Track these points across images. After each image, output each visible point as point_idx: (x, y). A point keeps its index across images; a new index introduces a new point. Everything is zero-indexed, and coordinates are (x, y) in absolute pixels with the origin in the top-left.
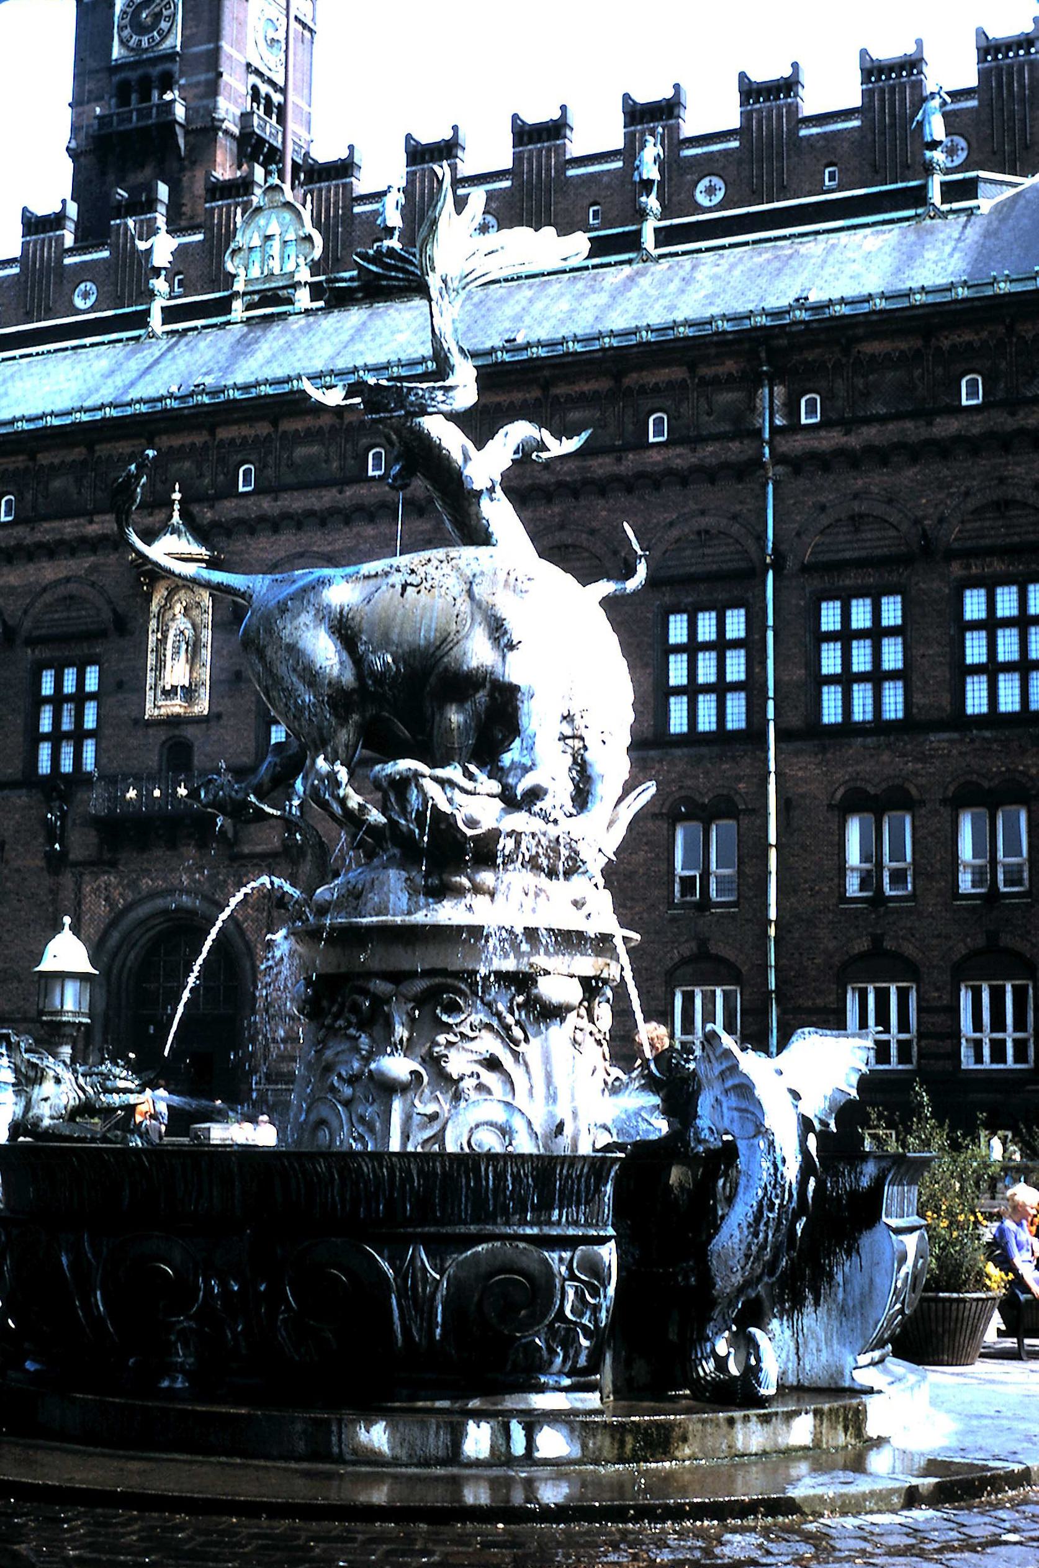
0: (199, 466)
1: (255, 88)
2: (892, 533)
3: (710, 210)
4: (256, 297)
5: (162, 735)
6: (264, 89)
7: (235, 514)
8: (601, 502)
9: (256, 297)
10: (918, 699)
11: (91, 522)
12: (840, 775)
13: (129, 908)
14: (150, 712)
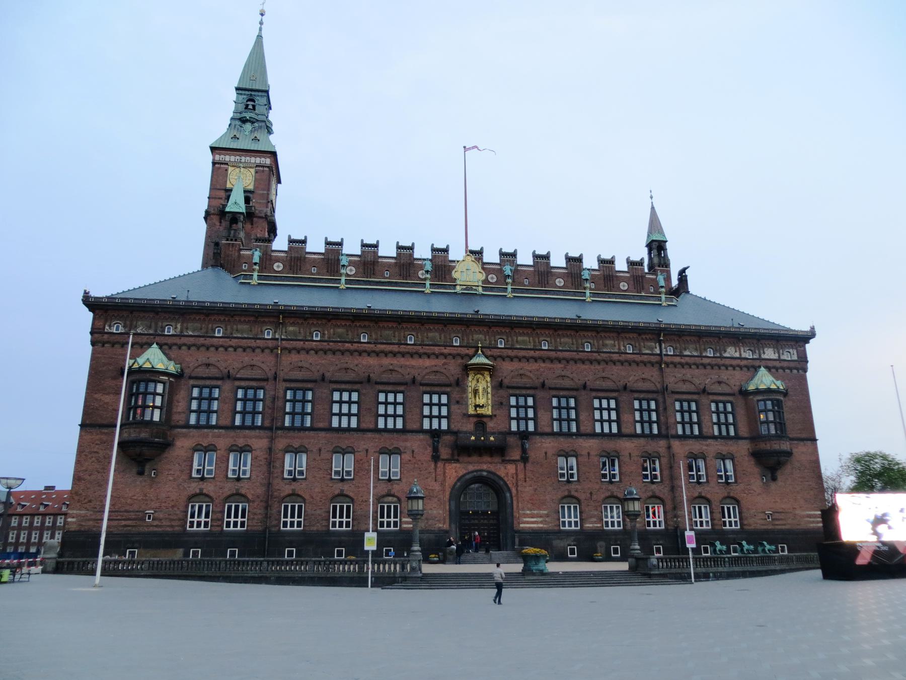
0: (485, 337)
2: (693, 386)
3: (560, 287)
4: (465, 287)
5: (475, 420)
7: (498, 354)
8: (614, 367)
9: (465, 287)
11: (445, 349)
12: (687, 448)
14: (471, 411)
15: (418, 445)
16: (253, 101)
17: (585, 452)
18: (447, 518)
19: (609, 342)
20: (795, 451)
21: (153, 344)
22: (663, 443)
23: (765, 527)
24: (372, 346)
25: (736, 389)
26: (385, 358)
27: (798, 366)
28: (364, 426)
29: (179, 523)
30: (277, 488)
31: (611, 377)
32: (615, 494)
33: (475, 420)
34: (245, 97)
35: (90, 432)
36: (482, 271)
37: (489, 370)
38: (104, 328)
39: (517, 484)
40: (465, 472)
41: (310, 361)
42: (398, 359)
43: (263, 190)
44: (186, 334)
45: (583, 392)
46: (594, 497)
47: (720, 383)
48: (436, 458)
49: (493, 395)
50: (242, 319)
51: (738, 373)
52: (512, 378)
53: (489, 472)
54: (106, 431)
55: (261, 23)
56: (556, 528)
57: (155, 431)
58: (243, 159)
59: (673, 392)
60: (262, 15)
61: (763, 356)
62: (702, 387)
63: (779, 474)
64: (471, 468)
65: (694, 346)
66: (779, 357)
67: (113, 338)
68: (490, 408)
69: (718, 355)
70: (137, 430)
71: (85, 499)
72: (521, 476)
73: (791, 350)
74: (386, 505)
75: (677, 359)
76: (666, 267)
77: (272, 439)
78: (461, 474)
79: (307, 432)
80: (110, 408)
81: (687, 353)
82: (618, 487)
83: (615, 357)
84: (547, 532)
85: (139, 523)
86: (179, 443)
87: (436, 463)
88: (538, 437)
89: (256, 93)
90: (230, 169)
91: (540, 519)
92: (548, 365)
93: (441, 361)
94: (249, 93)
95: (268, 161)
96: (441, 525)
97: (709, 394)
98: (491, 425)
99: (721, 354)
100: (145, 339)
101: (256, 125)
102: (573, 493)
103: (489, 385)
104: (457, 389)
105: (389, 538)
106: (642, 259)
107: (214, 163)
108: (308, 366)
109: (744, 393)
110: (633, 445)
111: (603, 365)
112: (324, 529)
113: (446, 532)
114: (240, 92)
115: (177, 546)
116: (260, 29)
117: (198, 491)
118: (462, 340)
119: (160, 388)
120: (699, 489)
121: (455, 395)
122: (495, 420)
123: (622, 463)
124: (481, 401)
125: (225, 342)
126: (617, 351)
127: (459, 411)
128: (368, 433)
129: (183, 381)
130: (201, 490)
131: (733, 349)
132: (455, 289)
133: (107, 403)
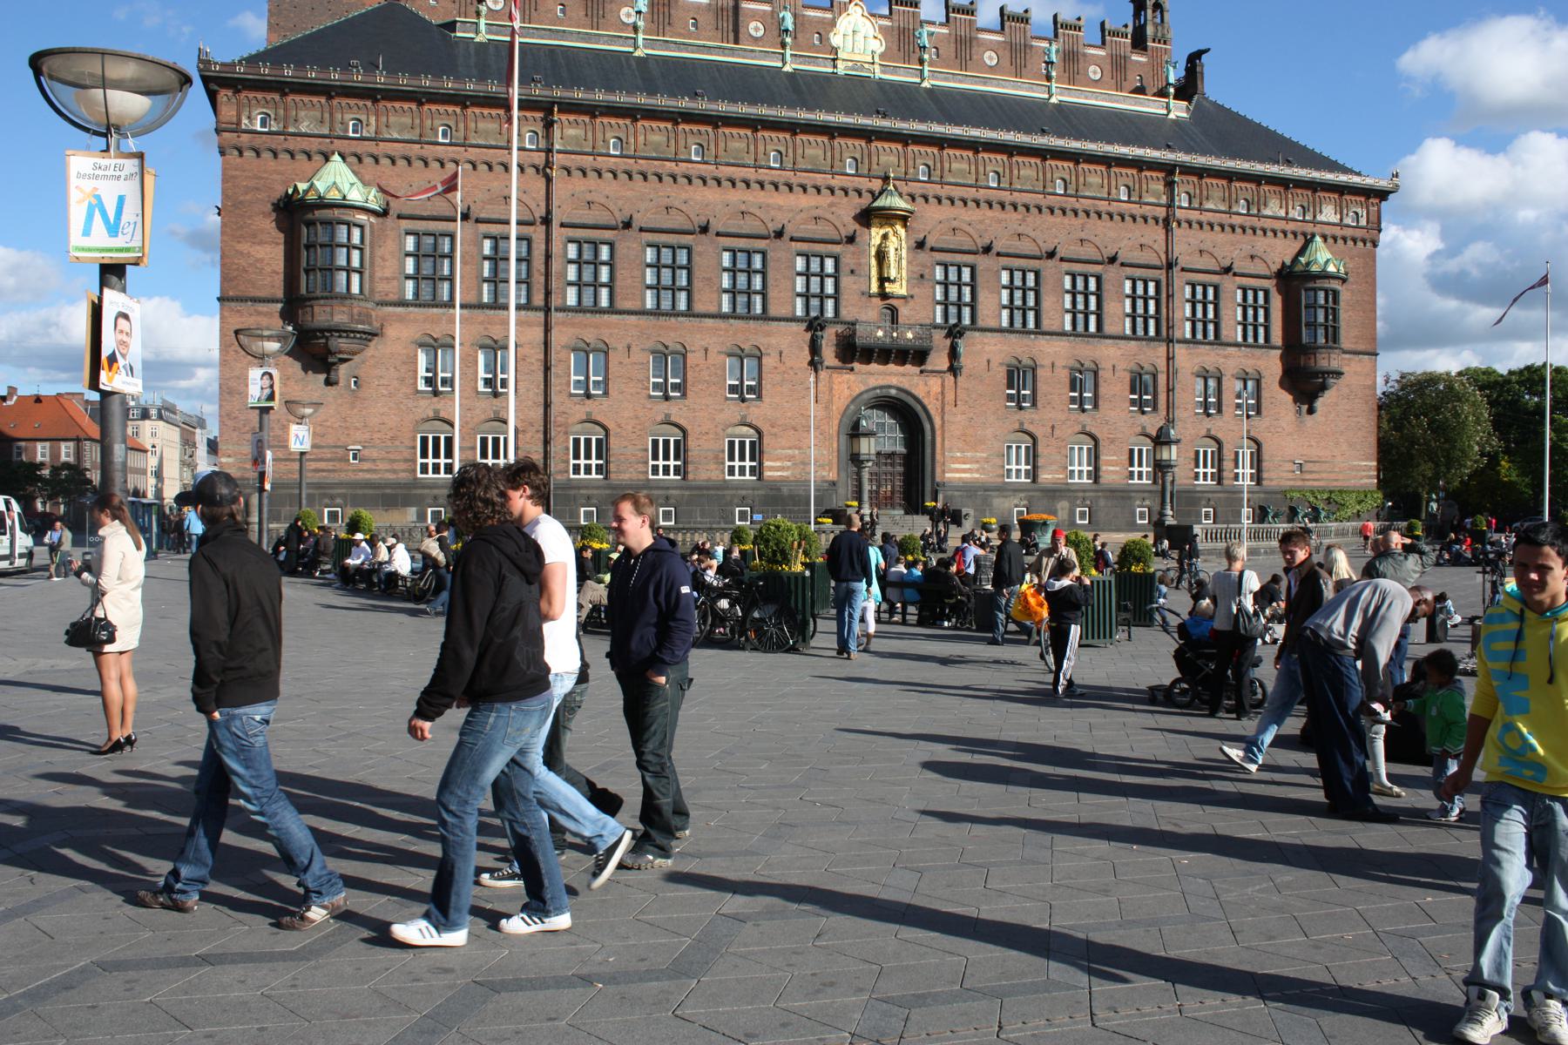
4: (850, 64)
13: (861, 394)
15: (788, 342)
17: (1047, 362)
18: (835, 460)
20: (1345, 369)
21: (333, 153)
23: (1292, 483)
24: (712, 168)
25: (1275, 267)
26: (732, 190)
27: (1367, 236)
28: (699, 307)
29: (403, 466)
30: (562, 409)
31: (1092, 238)
32: (1088, 429)
33: (877, 301)
35: (238, 311)
36: (880, 36)
37: (904, 220)
38: (239, 123)
39: (943, 409)
40: (863, 388)
41: (607, 193)
42: (755, 193)
44: (388, 136)
45: (1050, 263)
46: (1057, 432)
47: (1252, 257)
48: (815, 364)
49: (909, 263)
50: (486, 112)
51: (1280, 242)
53: (899, 389)
54: (265, 309)
56: (1000, 480)
57: (355, 311)
61: (1319, 218)
62: (1226, 263)
63: (1319, 404)
64: (873, 382)
66: (1341, 220)
67: (259, 142)
68: (904, 283)
69: (1255, 212)
70: (328, 309)
71: (244, 425)
72: (950, 397)
74: (737, 440)
76: (1165, 43)
77: (547, 329)
78: (857, 391)
79: (606, 316)
80: (268, 269)
81: (1210, 205)
82: (1094, 418)
83: (1103, 206)
84: (987, 488)
85: (338, 465)
86: (391, 332)
88: (977, 334)
91: (975, 466)
92: (996, 212)
93: (825, 199)
96: (825, 473)
97: (1235, 274)
98: (904, 312)
100: (314, 145)
102: (1027, 427)
103: (904, 244)
104: (851, 248)
105: (744, 492)
108: (603, 201)
110: (1119, 352)
112: (642, 477)
113: (834, 484)
115: (406, 502)
117: (431, 414)
120: (1207, 423)
121: (848, 261)
122: (911, 302)
123: (1101, 381)
125: (458, 153)
127: (855, 287)
128: (707, 320)
129: (390, 221)
130: (437, 412)
132: (835, 67)
133: (261, 260)
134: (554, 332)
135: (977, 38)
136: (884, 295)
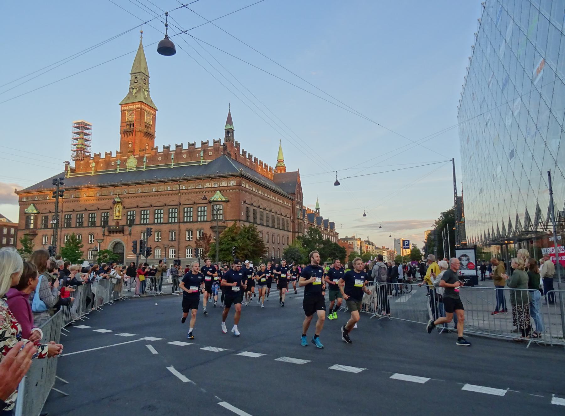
1: (146, 126)
6: (147, 125)
10: (194, 219)
14: (115, 219)
15: (99, 231)
16: (136, 78)
19: (161, 187)
22: (177, 225)
33: (116, 221)
34: (134, 77)
43: (138, 119)
48: (104, 235)
52: (129, 204)
55: (141, 37)
58: (131, 107)
59: (183, 205)
60: (142, 33)
61: (221, 186)
65: (193, 185)
66: (228, 184)
69: (202, 187)
73: (233, 181)
75: (186, 191)
76: (229, 141)
81: (190, 188)
87: (104, 236)
89: (139, 74)
90: (127, 112)
92: (140, 198)
93: (107, 201)
94: (134, 75)
95: (140, 106)
99: (203, 187)
101: (138, 89)
104: (111, 210)
106: (220, 139)
107: (121, 111)
109: (210, 202)
111: (159, 196)
114: (132, 75)
116: (141, 41)
118: (113, 193)
119: (32, 218)
120: (189, 243)
124: (117, 214)
126: (164, 190)
129: (39, 215)
131: (209, 184)
134: (62, 232)
135: (181, 152)
136: (116, 220)
